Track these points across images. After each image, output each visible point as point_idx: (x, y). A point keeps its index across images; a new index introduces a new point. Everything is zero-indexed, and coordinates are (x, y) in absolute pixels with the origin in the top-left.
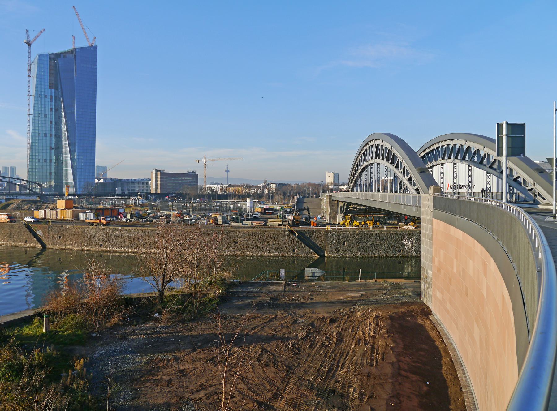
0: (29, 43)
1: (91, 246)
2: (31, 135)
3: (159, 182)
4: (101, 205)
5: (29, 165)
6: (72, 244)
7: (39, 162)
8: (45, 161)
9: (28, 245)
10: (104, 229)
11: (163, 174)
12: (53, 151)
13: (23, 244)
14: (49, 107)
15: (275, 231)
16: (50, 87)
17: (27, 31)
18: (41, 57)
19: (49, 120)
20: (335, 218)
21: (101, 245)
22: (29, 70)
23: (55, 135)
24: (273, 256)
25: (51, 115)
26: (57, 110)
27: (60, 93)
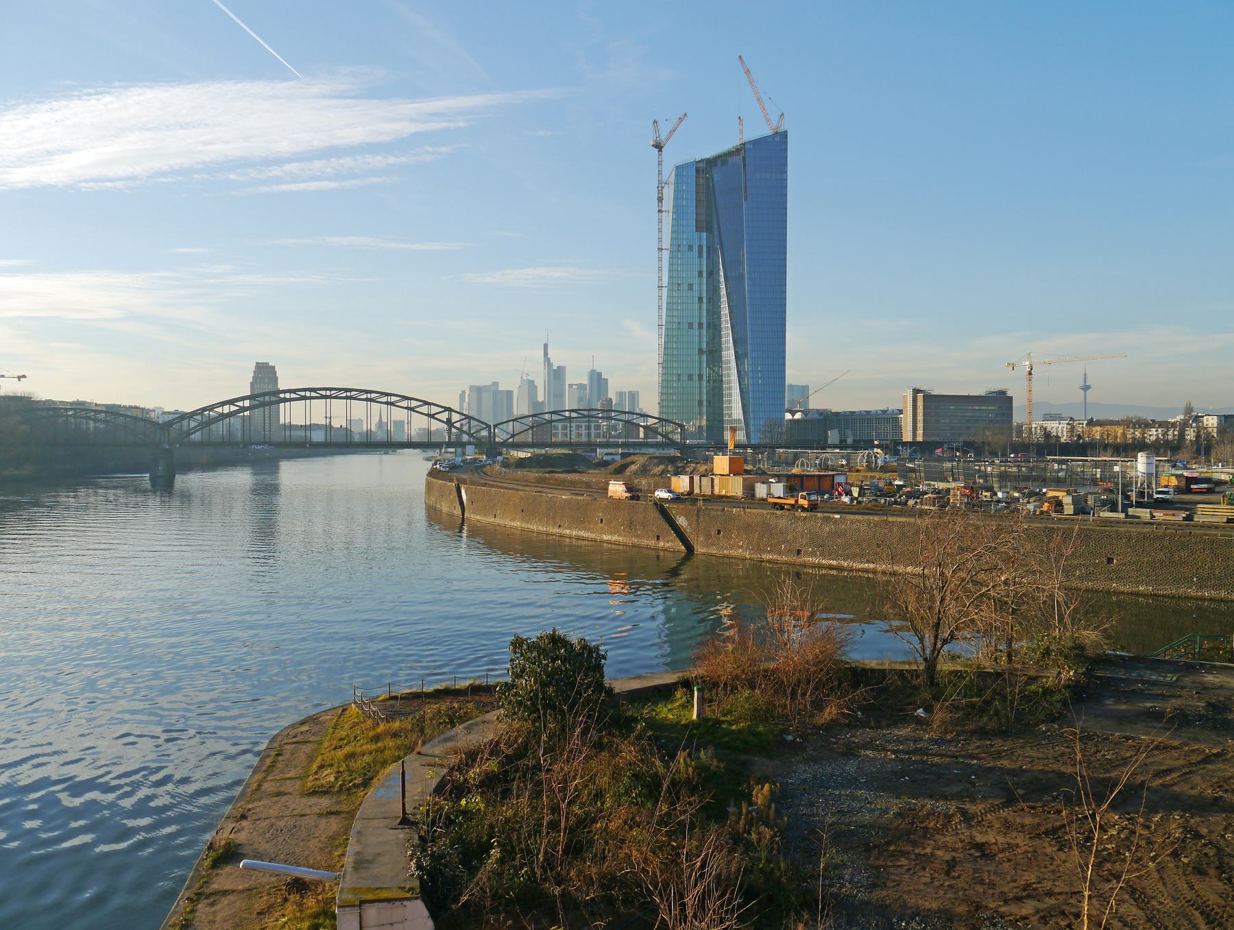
0: (659, 146)
1: (780, 553)
2: (664, 327)
3: (920, 418)
4: (798, 466)
5: (662, 387)
6: (741, 547)
7: (679, 380)
8: (690, 377)
9: (662, 544)
10: (805, 518)
11: (929, 398)
12: (704, 357)
13: (652, 543)
14: (697, 269)
15: (1216, 535)
16: (698, 229)
17: (655, 122)
18: (679, 169)
19: (697, 294)
21: (799, 552)
22: (660, 200)
23: (709, 325)
24: (1211, 600)
25: (700, 284)
26: (712, 274)
27: (717, 239)
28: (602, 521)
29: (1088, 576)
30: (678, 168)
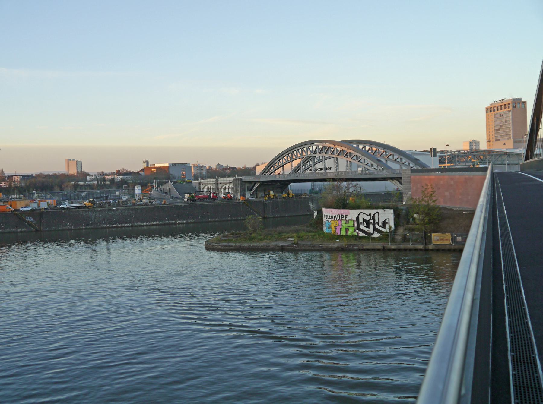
1: (90, 225)
6: (69, 225)
10: (100, 211)
20: (244, 195)
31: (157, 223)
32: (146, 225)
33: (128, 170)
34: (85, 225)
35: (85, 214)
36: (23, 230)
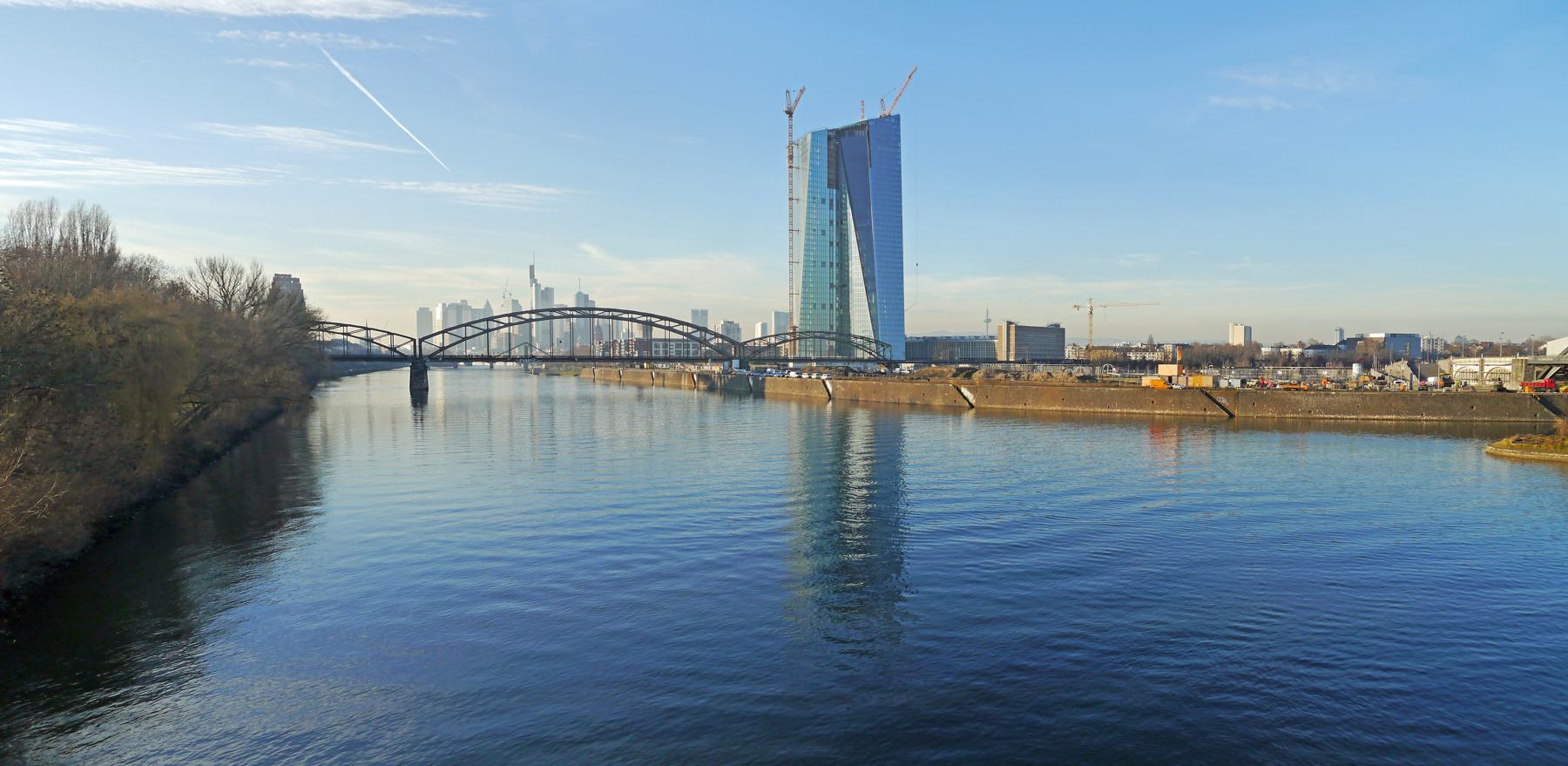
0: (790, 113)
1: (1298, 413)
3: (1013, 342)
7: (815, 308)
8: (824, 306)
10: (1313, 395)
11: (1018, 328)
16: (830, 186)
17: (787, 91)
21: (1310, 412)
22: (791, 157)
26: (841, 220)
28: (1153, 402)
29: (1464, 414)
30: (813, 133)
31: (1394, 417)
32: (1377, 420)
33: (1320, 342)
34: (1293, 412)
35: (1293, 397)
36: (1213, 414)
